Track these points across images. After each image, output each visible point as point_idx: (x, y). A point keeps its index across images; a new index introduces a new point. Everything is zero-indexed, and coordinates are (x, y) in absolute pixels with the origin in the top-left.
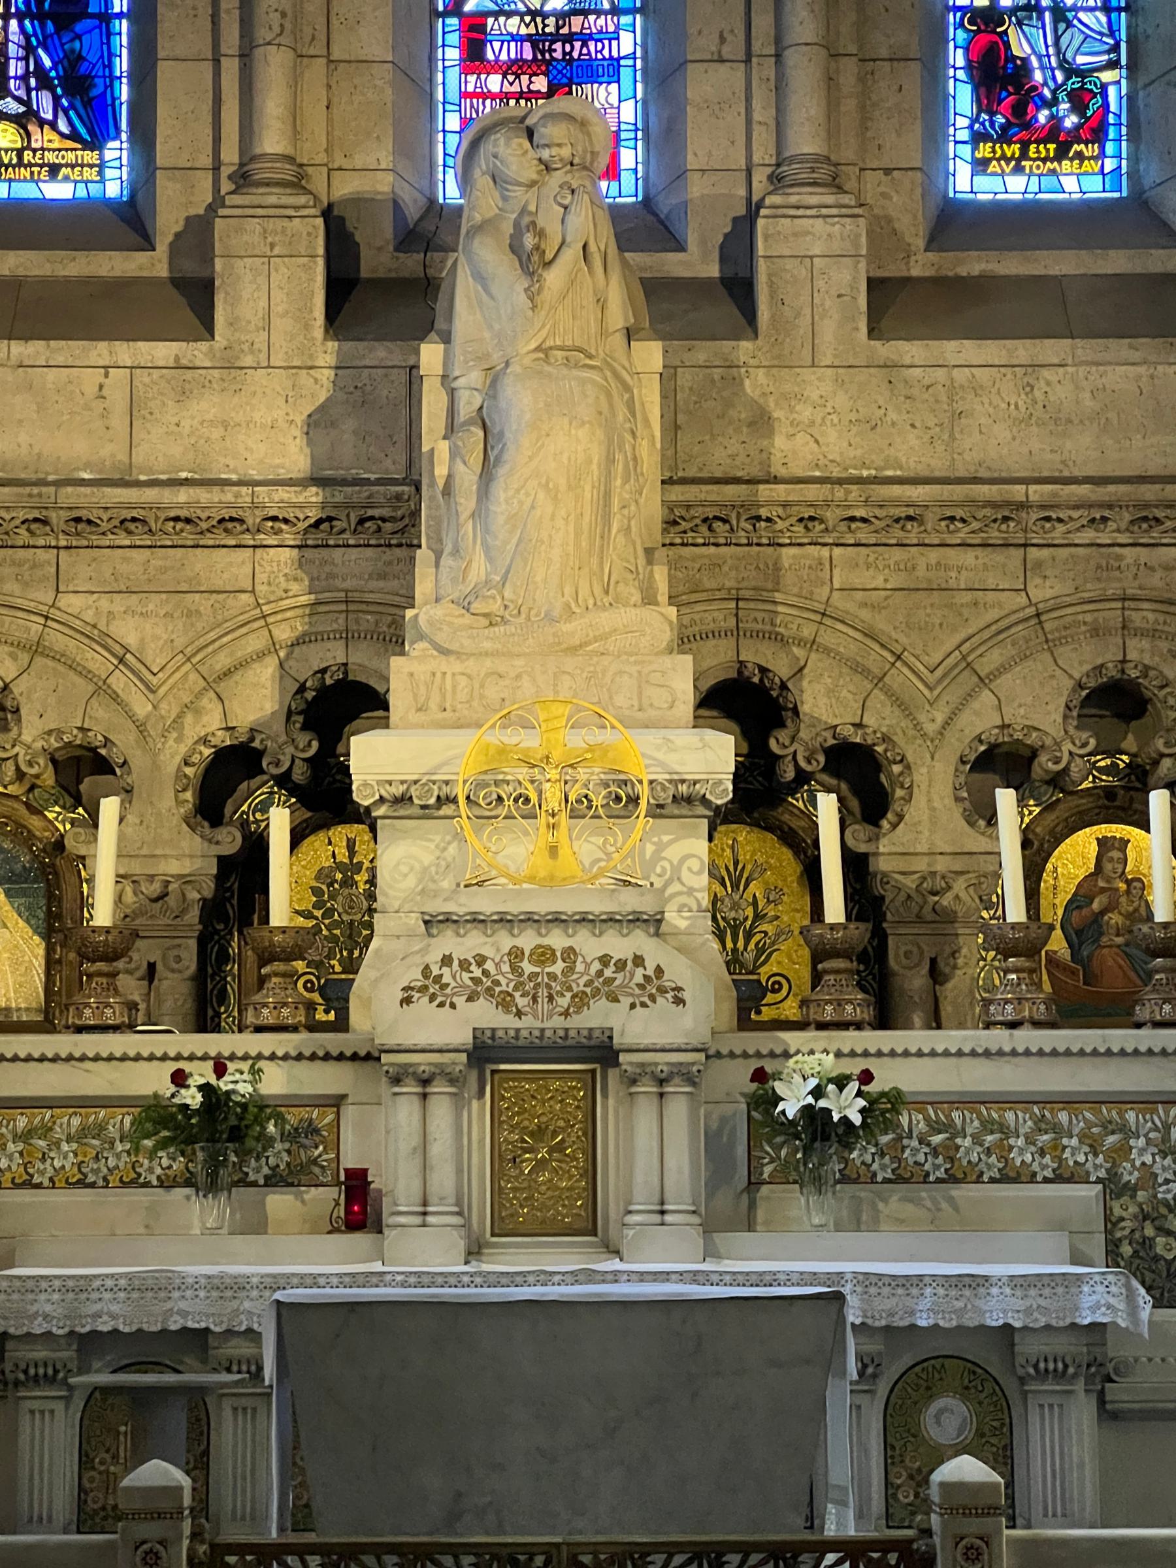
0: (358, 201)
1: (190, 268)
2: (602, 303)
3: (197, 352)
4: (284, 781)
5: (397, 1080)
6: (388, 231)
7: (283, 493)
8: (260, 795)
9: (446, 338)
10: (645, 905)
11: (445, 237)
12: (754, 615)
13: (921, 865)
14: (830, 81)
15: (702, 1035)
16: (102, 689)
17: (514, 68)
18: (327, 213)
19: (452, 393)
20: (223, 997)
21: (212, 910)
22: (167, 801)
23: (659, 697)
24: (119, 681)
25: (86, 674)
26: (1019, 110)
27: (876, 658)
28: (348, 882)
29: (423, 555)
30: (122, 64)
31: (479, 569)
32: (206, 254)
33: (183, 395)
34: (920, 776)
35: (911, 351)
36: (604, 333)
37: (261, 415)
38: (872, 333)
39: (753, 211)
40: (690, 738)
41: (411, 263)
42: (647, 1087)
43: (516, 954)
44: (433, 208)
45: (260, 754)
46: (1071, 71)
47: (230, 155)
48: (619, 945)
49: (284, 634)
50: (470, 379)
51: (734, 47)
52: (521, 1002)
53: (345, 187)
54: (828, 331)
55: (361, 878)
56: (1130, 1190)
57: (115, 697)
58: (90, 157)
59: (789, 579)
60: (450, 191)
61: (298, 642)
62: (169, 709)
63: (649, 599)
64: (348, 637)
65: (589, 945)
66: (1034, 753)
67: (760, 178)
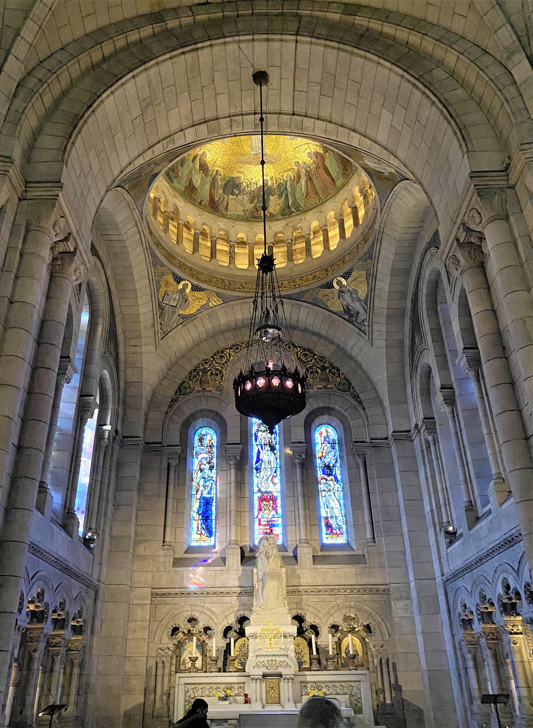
0: (245, 546)
1: (223, 556)
2: (277, 562)
3: (224, 568)
4: (235, 631)
5: (252, 680)
6: (249, 549)
7: (235, 589)
8: (232, 633)
9: (257, 568)
10: (286, 653)
11: (257, 551)
12: (299, 606)
13: (324, 643)
14: (306, 528)
15: (294, 673)
16: (211, 618)
17: (265, 525)
18: (241, 548)
19: (258, 576)
20: (227, 665)
21: (225, 651)
22: (219, 635)
23: (286, 620)
24: (213, 617)
25: (208, 616)
26: (332, 530)
27: (316, 612)
28: (244, 647)
29: (254, 599)
30: (213, 526)
31: (262, 601)
32: (225, 554)
33: (222, 575)
34: (323, 630)
35: (319, 567)
36: (278, 567)
37: (232, 577)
38: (314, 564)
39: (297, 546)
40: (290, 627)
41: (252, 554)
42: (286, 681)
43: (268, 661)
44: (254, 546)
45: (232, 627)
46: (338, 525)
47: (228, 540)
48: (282, 659)
49: (235, 609)
50: (261, 574)
51: (294, 524)
52: (269, 668)
53: (243, 544)
54: (308, 565)
55: (246, 646)
56: (353, 696)
57: (212, 619)
58: (209, 539)
59: (304, 601)
60: (256, 543)
61: (238, 611)
62: (220, 621)
63: (285, 606)
64: (244, 610)
65: (278, 659)
66: (339, 626)
67: (298, 543)
